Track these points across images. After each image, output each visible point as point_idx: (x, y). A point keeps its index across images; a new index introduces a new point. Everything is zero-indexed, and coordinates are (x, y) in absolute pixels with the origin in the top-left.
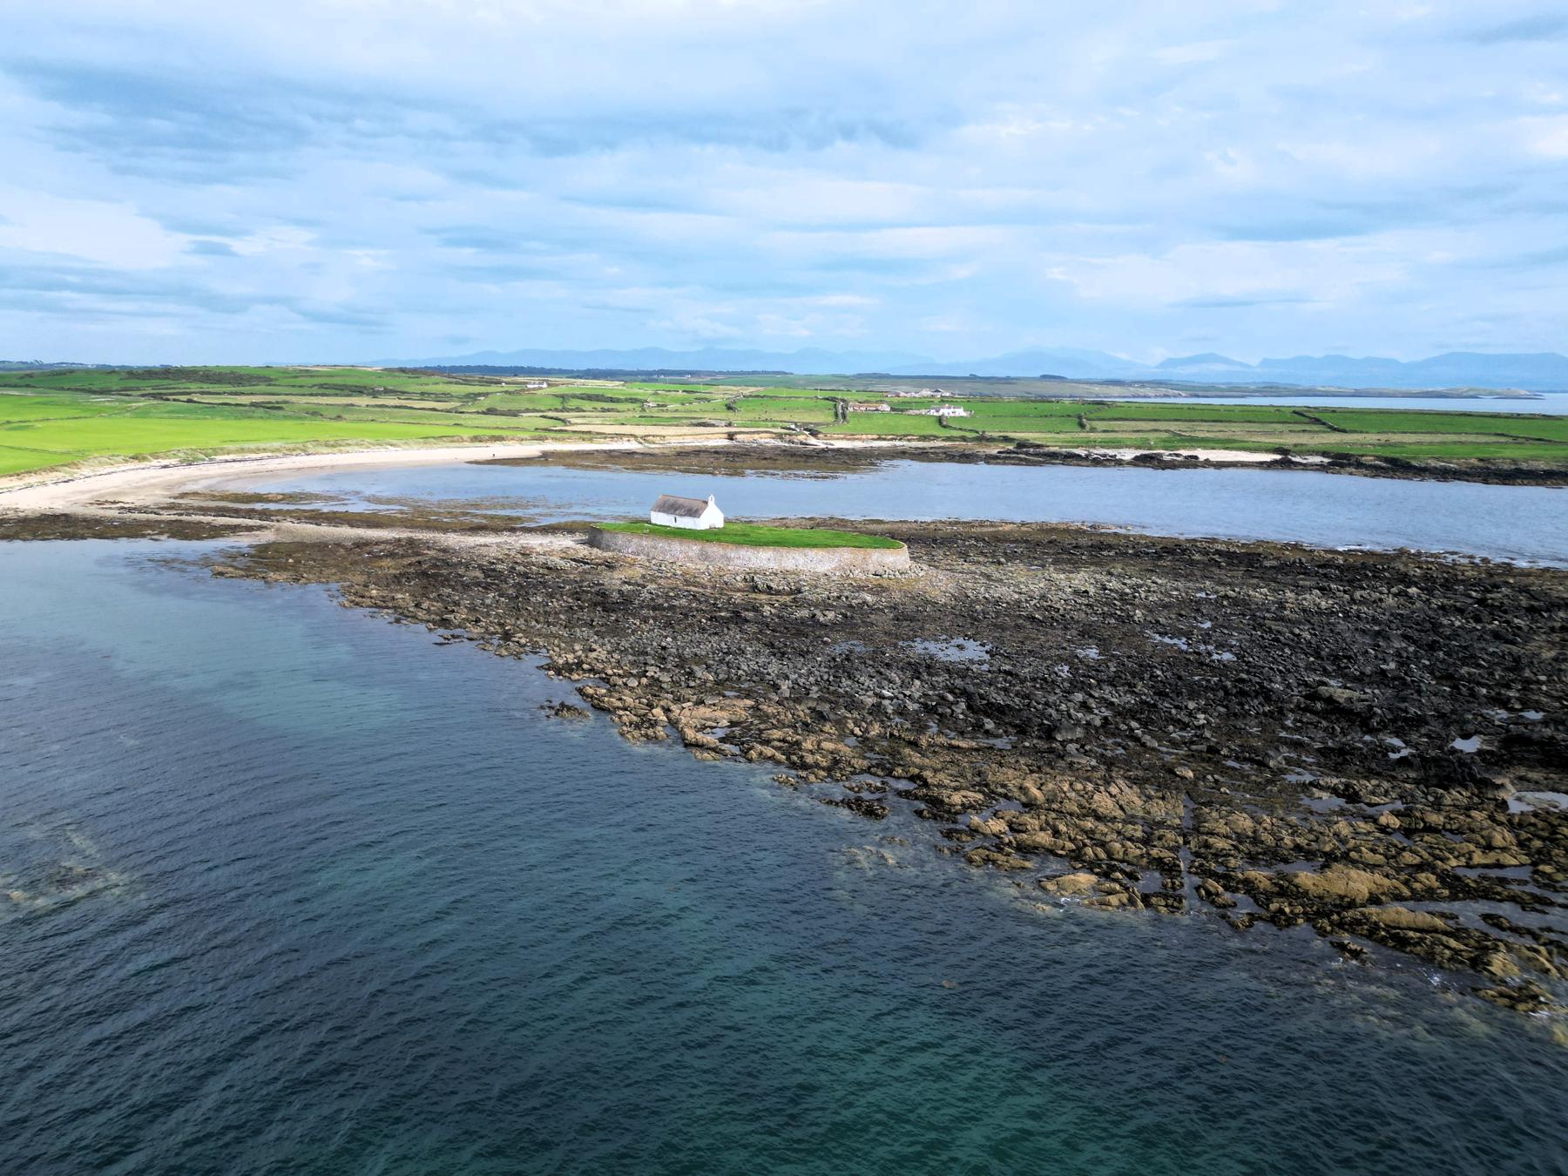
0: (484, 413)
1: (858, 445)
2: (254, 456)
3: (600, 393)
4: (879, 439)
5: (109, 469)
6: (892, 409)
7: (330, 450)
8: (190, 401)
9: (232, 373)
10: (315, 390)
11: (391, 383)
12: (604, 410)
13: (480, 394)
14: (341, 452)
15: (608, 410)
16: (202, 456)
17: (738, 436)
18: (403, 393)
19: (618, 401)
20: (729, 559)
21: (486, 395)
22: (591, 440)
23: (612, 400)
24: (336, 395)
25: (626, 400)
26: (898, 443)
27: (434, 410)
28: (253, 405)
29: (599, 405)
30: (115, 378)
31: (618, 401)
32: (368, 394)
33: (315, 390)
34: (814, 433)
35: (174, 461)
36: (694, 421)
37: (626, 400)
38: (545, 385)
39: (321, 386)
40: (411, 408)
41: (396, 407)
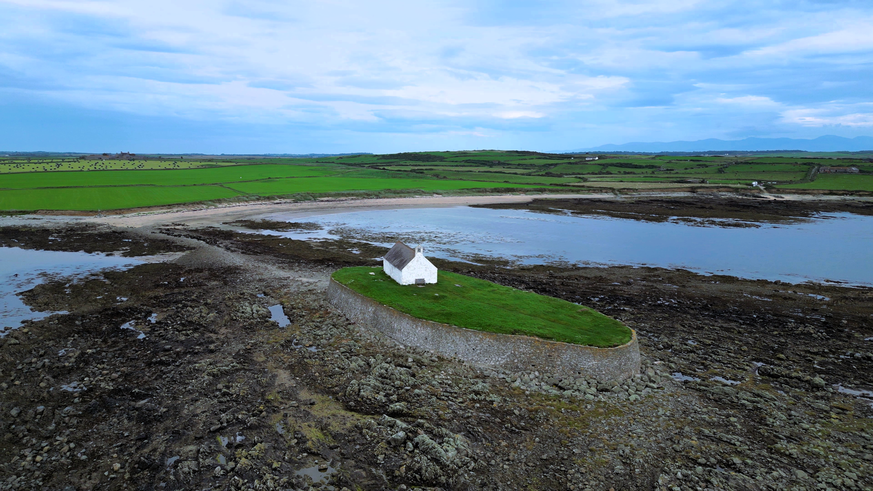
0: (542, 175)
1: (809, 198)
2: (343, 198)
3: (630, 162)
4: (831, 193)
5: (238, 204)
6: (861, 171)
7: (394, 195)
8: (384, 169)
9: (426, 154)
10: (463, 164)
11: (502, 160)
12: (625, 173)
13: (552, 165)
14: (401, 197)
15: (628, 173)
16: (311, 198)
17: (699, 190)
18: (508, 164)
19: (641, 167)
20: (392, 330)
21: (556, 165)
22: (578, 192)
23: (636, 167)
24: (471, 166)
25: (647, 167)
26: (848, 197)
27: (516, 174)
28: (412, 171)
29: (623, 170)
30: (376, 158)
31: (641, 167)
32: (488, 165)
33: (463, 164)
34: (769, 189)
35: (288, 200)
36: (675, 180)
37: (647, 167)
38: (597, 158)
39: (466, 161)
40: (504, 173)
41: (485, 172)
